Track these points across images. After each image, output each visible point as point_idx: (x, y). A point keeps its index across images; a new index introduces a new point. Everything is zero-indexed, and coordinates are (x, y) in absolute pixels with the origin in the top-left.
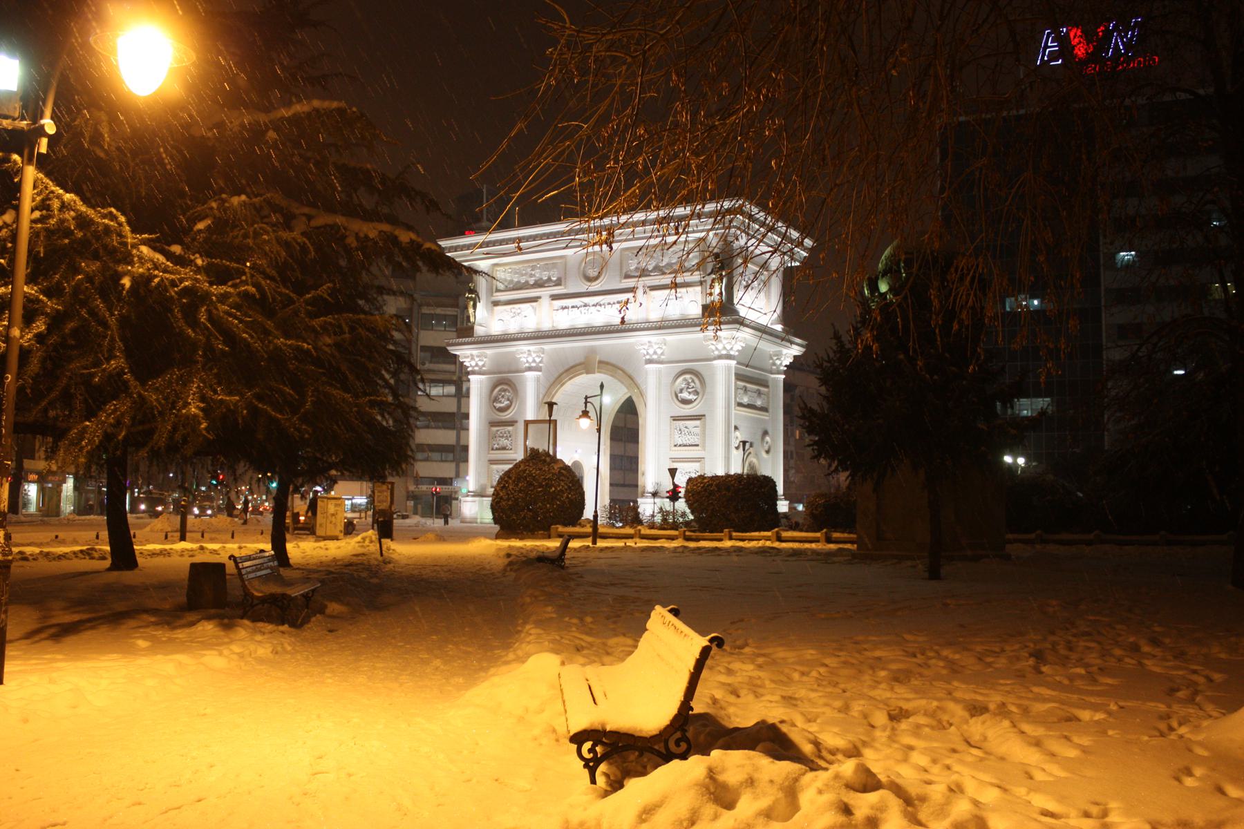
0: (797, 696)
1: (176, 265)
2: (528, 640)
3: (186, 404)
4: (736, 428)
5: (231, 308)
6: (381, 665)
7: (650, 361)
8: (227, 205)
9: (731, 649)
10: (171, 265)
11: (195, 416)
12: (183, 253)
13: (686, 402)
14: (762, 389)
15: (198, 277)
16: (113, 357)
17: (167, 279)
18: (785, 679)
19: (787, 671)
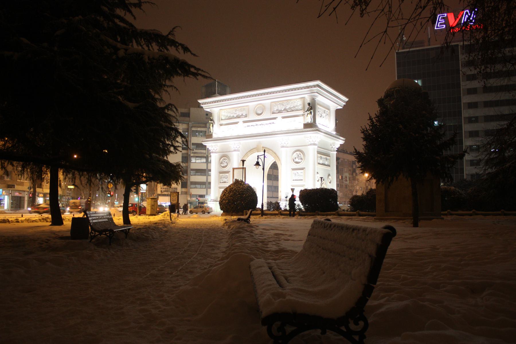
4: (317, 173)
7: (283, 147)
13: (297, 163)
14: (328, 158)
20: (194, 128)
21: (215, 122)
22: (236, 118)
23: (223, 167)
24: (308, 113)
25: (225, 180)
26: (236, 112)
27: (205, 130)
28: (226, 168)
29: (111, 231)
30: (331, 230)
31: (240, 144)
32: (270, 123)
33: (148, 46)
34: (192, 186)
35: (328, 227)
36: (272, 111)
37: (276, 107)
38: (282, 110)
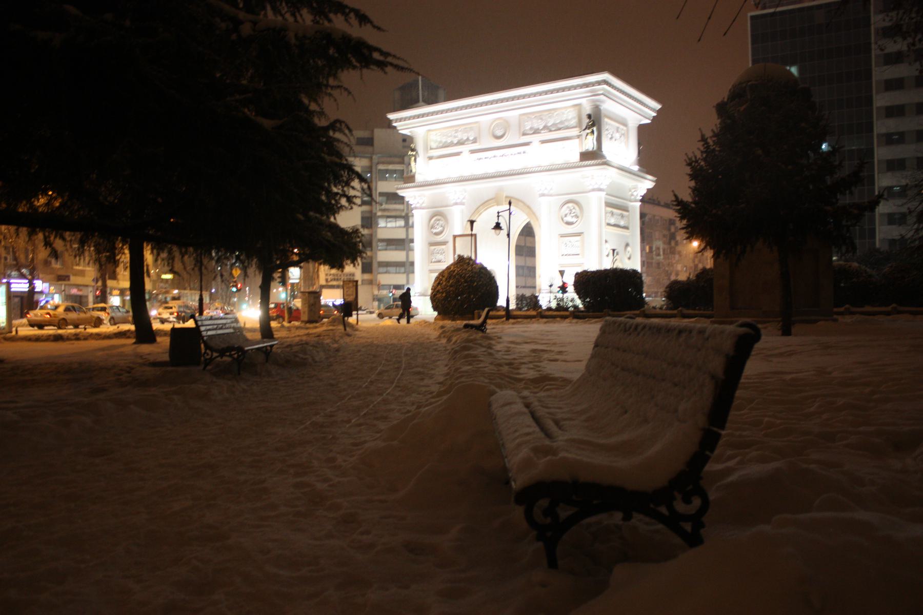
4: (606, 241)
7: (543, 195)
13: (568, 223)
14: (625, 213)
20: (381, 165)
21: (419, 152)
23: (437, 234)
24: (587, 135)
25: (439, 257)
26: (456, 134)
27: (402, 168)
28: (441, 236)
29: (240, 349)
30: (638, 334)
31: (465, 192)
32: (518, 153)
33: (293, 15)
34: (382, 270)
35: (631, 330)
36: (522, 130)
37: (530, 123)
38: (540, 129)
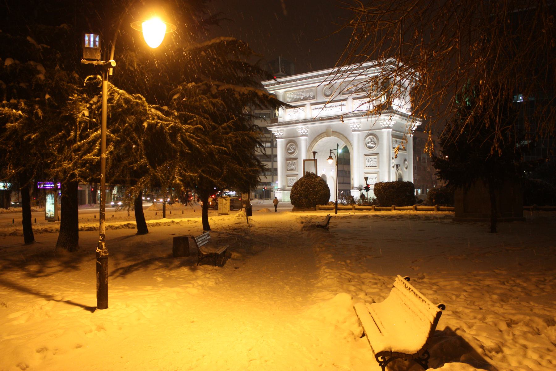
0: (458, 310)
1: (167, 117)
2: (326, 275)
3: (174, 178)
5: (191, 134)
6: (263, 290)
7: (354, 131)
8: (186, 87)
9: (418, 279)
10: (165, 116)
11: (179, 184)
12: (168, 110)
15: (177, 121)
16: (141, 158)
17: (164, 124)
18: (449, 299)
19: (448, 294)
22: (302, 100)
25: (292, 167)
26: (302, 94)
28: (294, 154)
32: (340, 105)
